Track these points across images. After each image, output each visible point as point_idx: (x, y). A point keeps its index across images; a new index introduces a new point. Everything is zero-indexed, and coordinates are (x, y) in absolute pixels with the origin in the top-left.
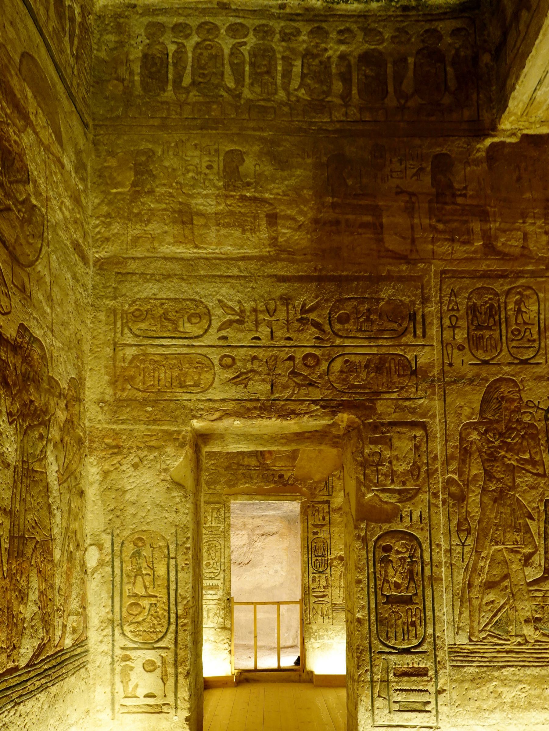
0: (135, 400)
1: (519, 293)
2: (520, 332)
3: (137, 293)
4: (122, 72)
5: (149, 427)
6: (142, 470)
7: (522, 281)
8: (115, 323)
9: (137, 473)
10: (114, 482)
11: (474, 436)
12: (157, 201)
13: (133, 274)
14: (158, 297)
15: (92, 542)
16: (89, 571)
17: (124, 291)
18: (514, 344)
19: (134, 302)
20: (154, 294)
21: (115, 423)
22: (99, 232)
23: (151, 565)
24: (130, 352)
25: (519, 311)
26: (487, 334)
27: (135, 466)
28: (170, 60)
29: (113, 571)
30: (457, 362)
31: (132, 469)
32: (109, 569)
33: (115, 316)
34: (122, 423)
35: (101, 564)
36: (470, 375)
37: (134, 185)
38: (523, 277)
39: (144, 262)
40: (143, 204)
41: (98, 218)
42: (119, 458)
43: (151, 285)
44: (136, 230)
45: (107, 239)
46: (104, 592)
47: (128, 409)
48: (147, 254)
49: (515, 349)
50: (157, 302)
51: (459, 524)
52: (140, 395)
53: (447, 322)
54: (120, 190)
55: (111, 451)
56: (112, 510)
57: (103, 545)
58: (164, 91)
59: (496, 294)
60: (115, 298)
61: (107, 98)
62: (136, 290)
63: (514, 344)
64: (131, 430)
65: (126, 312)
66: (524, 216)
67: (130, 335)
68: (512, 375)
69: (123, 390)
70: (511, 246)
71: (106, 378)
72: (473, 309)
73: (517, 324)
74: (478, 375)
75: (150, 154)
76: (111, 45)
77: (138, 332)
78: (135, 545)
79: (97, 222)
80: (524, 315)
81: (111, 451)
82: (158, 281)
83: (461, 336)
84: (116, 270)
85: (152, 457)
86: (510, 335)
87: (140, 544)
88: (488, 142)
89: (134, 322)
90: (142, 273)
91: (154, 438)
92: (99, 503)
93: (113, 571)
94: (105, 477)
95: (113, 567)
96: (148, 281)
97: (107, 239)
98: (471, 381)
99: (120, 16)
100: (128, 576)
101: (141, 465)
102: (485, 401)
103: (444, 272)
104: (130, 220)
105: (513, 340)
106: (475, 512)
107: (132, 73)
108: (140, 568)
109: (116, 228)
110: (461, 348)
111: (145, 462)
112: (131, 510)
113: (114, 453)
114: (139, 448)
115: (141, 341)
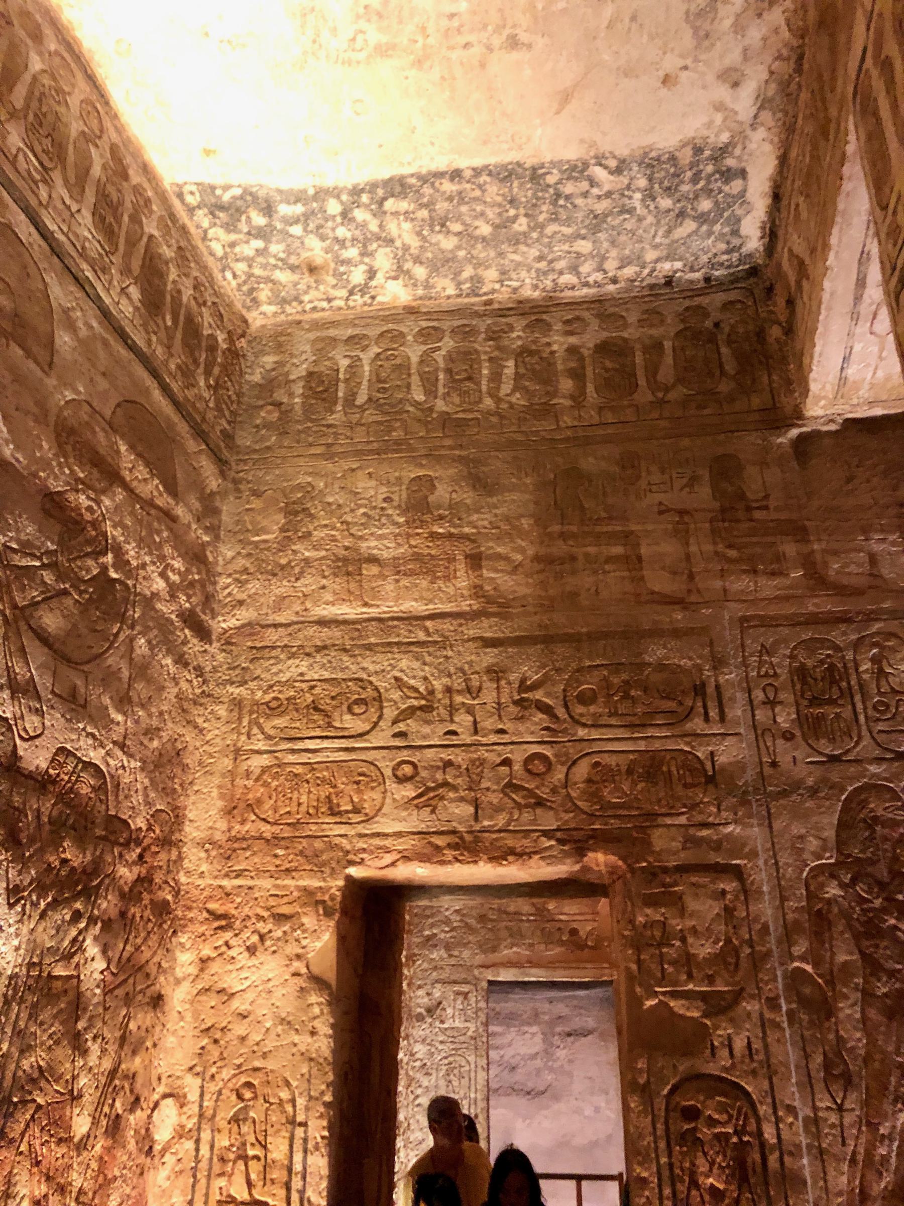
0: (260, 838)
1: (876, 645)
2: (888, 706)
3: (276, 674)
4: (280, 395)
5: (279, 882)
6: (261, 956)
7: (877, 626)
8: (240, 719)
9: (254, 961)
10: (215, 978)
11: (833, 890)
12: (315, 548)
13: (274, 648)
14: (307, 678)
15: (168, 1091)
16: (157, 1148)
17: (258, 672)
18: (881, 726)
19: (271, 687)
20: (302, 674)
21: (227, 875)
22: (230, 594)
23: (261, 1138)
24: (257, 762)
25: (881, 674)
26: (831, 712)
27: (251, 950)
28: (341, 376)
29: (197, 1150)
30: (785, 761)
31: (246, 954)
32: (189, 1145)
33: (240, 709)
34: (237, 877)
35: (181, 1133)
36: (810, 781)
37: (283, 530)
38: (877, 620)
39: (290, 629)
40: (295, 552)
41: (230, 575)
42: (228, 935)
43: (297, 661)
44: (281, 587)
45: (241, 603)
46: (177, 1192)
47: (248, 853)
48: (295, 619)
49: (884, 736)
50: (304, 686)
51: (827, 1066)
52: (267, 830)
53: (759, 695)
54: (264, 537)
55: (216, 924)
56: (208, 1029)
57: (185, 1096)
58: (332, 412)
59: (837, 648)
60: (243, 683)
61: (257, 426)
62: (274, 669)
63: (881, 726)
64: (250, 888)
65: (257, 703)
66: (866, 530)
67: (261, 736)
68: (886, 779)
69: (243, 822)
70: (849, 574)
71: (220, 804)
72: (801, 674)
73: (880, 693)
74: (824, 780)
75: (308, 490)
76: (268, 367)
77: (272, 732)
78: (240, 1097)
79: (229, 580)
80: (891, 679)
81: (216, 924)
82: (308, 655)
83: (785, 718)
84: (249, 644)
85: (279, 933)
86: (870, 712)
87: (248, 1095)
88: (794, 432)
89: (268, 717)
90: (286, 646)
91: (285, 900)
92: (188, 1017)
93: (197, 1150)
94: (202, 970)
95: (197, 1141)
96: (293, 656)
97: (241, 603)
98: (814, 792)
99: (281, 334)
100: (222, 1160)
101: (260, 949)
102: (842, 826)
103: (744, 619)
104: (275, 575)
105: (878, 720)
106: (856, 1039)
107: (291, 395)
108: (244, 1144)
109: (254, 586)
110: (788, 736)
111: (268, 943)
112: (240, 1029)
113: (221, 928)
114: (260, 918)
115: (276, 744)
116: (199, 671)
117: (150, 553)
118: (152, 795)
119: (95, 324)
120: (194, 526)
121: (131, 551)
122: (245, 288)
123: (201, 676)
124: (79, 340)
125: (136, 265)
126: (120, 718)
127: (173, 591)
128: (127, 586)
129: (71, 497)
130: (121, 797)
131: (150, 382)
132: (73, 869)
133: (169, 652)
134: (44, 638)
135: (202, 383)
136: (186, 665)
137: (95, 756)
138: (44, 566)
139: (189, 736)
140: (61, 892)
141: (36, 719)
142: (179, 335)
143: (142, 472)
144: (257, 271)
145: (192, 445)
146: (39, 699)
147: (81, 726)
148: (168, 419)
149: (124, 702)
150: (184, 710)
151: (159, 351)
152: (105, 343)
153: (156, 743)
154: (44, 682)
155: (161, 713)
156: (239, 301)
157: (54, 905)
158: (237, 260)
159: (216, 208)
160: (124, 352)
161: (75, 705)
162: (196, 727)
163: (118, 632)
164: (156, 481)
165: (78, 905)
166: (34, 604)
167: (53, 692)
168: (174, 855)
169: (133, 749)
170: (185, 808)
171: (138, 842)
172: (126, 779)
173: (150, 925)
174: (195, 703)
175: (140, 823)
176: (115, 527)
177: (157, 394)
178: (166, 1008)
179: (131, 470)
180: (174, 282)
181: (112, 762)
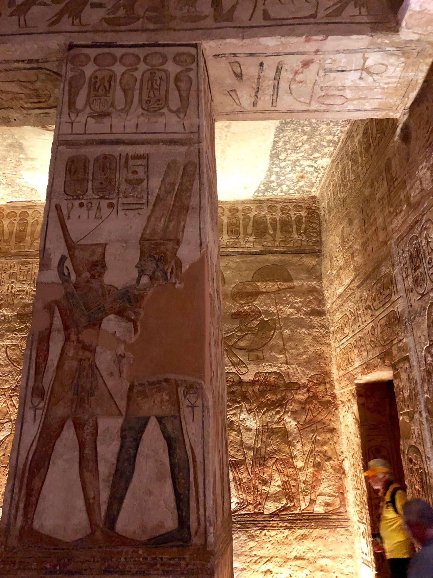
116: (322, 326)
117: (282, 304)
118: (307, 372)
119: (238, 260)
120: (305, 284)
121: (273, 309)
122: (301, 192)
123: (324, 327)
124: (233, 269)
125: (250, 231)
126: (281, 356)
127: (298, 310)
128: (274, 319)
129: (241, 310)
130: (291, 377)
131: (266, 257)
132: (273, 401)
133: (302, 329)
134: (242, 349)
135: (296, 236)
136: (314, 327)
137: (274, 369)
138: (236, 332)
139: (324, 348)
140: (270, 407)
141: (245, 369)
142: (278, 232)
143: (270, 284)
144: (296, 188)
145: (295, 259)
146: (244, 363)
147: (264, 364)
148: (281, 261)
149: (283, 351)
150: (318, 341)
151: (269, 245)
152: (243, 262)
153: (304, 356)
154: (244, 359)
155: (305, 347)
156: (305, 196)
157: (268, 411)
158: (288, 191)
159: (266, 190)
160: (253, 258)
161: (258, 360)
162: (326, 344)
163: (274, 333)
164: (278, 283)
165: (278, 409)
166: (236, 342)
167: (249, 360)
168: (328, 386)
169: (291, 362)
170: (330, 370)
171: (304, 387)
172: (291, 371)
173: (320, 409)
174: (323, 337)
175: (304, 381)
176: (262, 307)
177: (272, 258)
178: (338, 432)
179: (265, 288)
180: (270, 218)
181: (282, 369)
